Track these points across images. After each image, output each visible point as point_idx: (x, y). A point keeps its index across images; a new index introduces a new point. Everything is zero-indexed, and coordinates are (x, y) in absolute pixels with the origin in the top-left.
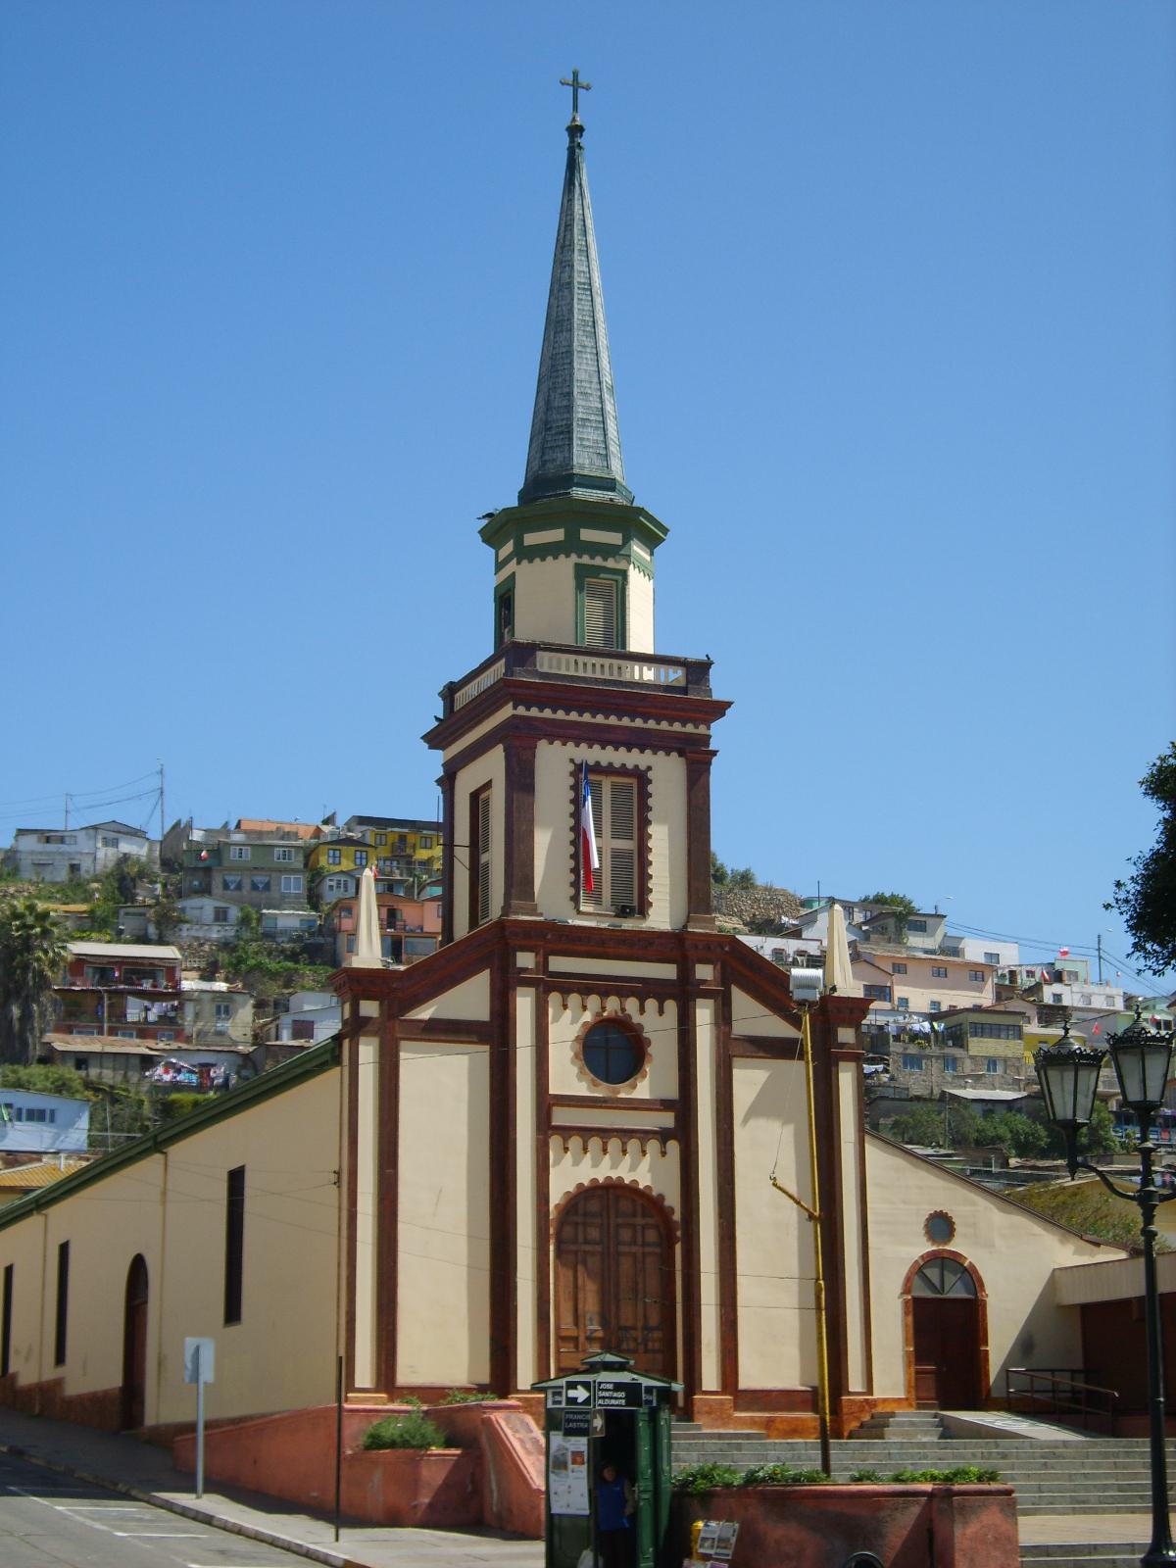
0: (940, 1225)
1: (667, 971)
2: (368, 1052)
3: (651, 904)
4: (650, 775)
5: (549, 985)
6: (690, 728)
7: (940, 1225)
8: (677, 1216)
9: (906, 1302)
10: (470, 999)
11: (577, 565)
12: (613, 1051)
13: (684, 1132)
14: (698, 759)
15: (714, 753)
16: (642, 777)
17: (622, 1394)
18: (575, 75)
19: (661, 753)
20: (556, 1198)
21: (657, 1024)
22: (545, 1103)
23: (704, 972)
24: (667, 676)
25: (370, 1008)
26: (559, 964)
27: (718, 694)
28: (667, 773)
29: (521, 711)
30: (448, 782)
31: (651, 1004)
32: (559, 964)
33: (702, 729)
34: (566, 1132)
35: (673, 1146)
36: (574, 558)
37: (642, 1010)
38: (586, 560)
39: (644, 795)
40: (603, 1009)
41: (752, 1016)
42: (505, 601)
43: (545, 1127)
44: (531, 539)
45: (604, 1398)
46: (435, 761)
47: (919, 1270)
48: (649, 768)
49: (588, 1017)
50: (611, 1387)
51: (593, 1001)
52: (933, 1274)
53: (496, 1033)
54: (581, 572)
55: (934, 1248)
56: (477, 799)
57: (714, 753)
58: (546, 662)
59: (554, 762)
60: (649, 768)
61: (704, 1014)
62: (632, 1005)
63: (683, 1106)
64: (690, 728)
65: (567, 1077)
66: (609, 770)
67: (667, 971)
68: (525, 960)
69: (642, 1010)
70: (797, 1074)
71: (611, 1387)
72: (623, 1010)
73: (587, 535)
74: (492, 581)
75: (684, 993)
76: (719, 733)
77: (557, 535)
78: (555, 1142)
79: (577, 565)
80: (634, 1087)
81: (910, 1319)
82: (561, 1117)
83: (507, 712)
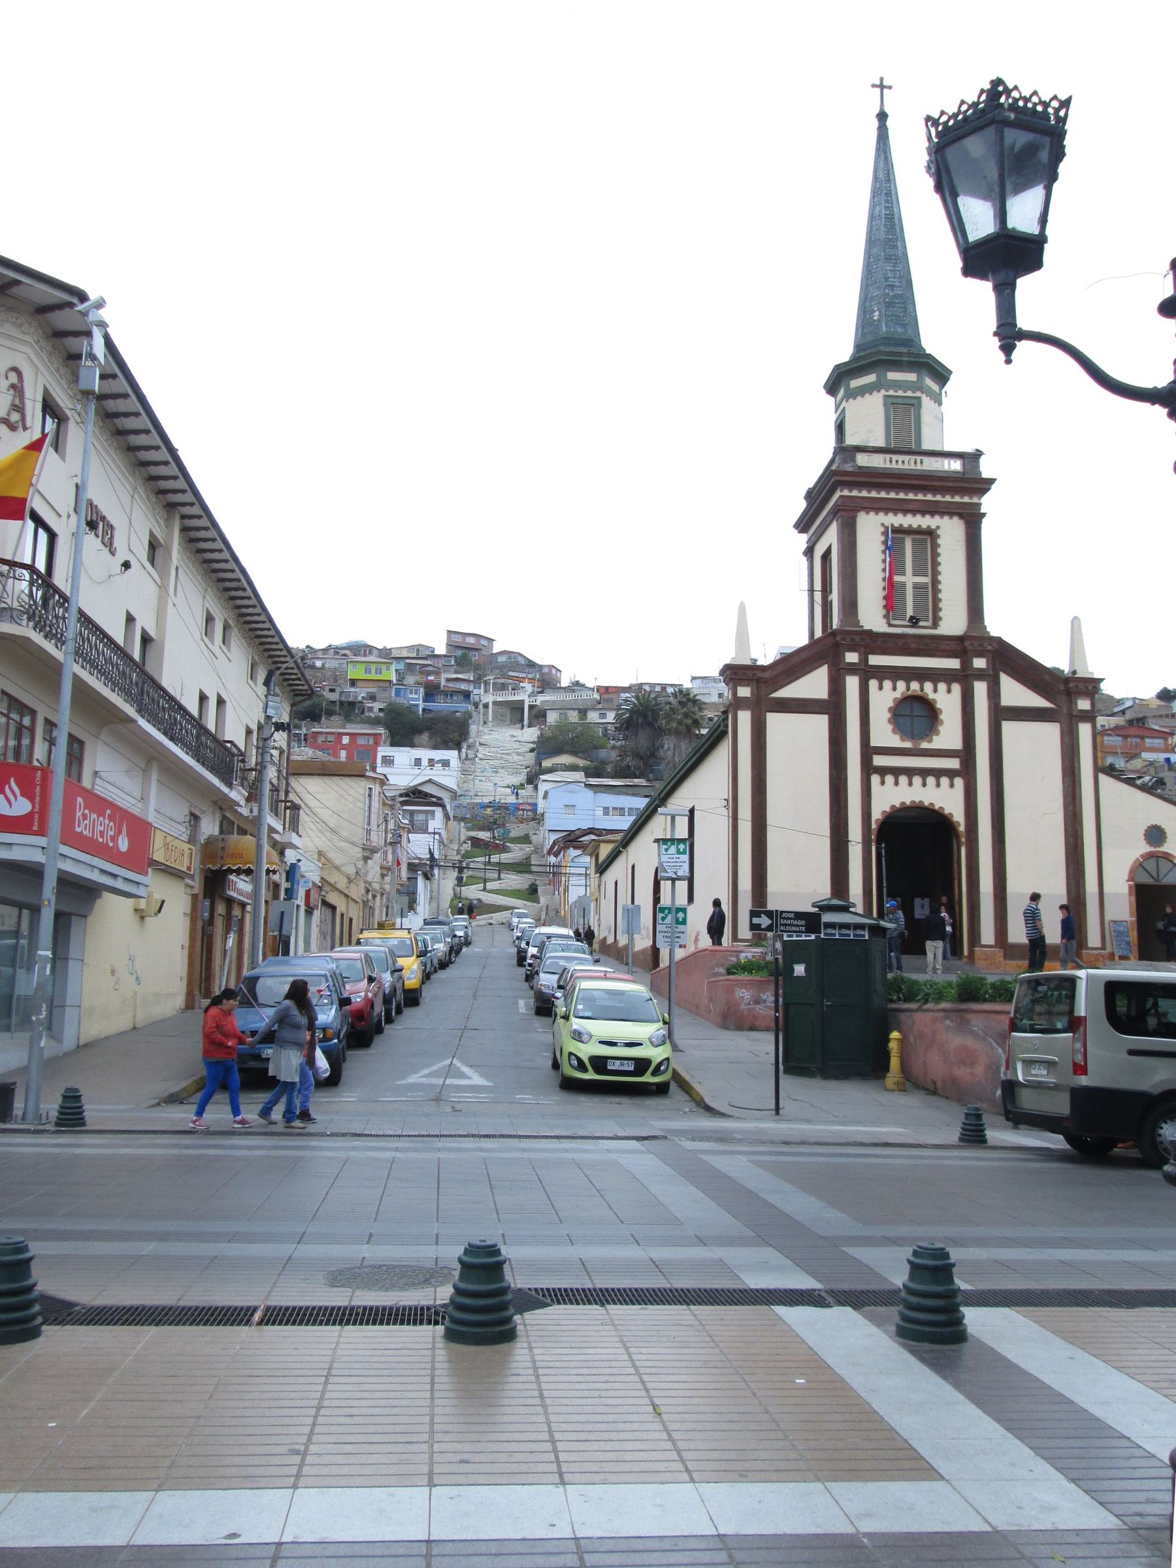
0: (1155, 834)
1: (954, 664)
2: (744, 718)
3: (941, 619)
4: (939, 532)
5: (867, 673)
6: (966, 499)
7: (1155, 834)
8: (962, 828)
9: (1130, 887)
10: (814, 684)
11: (886, 397)
12: (917, 715)
13: (968, 771)
14: (973, 520)
15: (984, 515)
16: (931, 534)
17: (803, 922)
18: (882, 79)
19: (946, 518)
20: (877, 815)
21: (947, 700)
22: (868, 751)
23: (980, 663)
24: (949, 464)
25: (744, 692)
26: (875, 660)
27: (985, 474)
28: (950, 531)
29: (846, 493)
30: (809, 552)
31: (942, 687)
32: (875, 660)
33: (975, 500)
34: (883, 771)
35: (959, 782)
36: (883, 392)
37: (935, 691)
38: (891, 393)
39: (935, 546)
40: (908, 689)
41: (1014, 693)
42: (840, 428)
43: (868, 769)
44: (855, 383)
45: (785, 925)
46: (802, 540)
47: (1139, 866)
48: (938, 527)
49: (898, 694)
50: (792, 915)
51: (901, 685)
52: (1151, 865)
53: (833, 707)
54: (889, 402)
55: (1152, 849)
56: (826, 556)
57: (984, 515)
58: (863, 460)
59: (870, 530)
60: (938, 527)
61: (980, 689)
62: (928, 687)
63: (967, 753)
64: (966, 499)
65: (883, 734)
66: (910, 531)
67: (954, 664)
68: (852, 657)
69: (935, 691)
70: (1050, 733)
71: (792, 915)
72: (922, 689)
73: (892, 376)
74: (832, 417)
75: (965, 678)
76: (988, 503)
77: (871, 378)
78: (875, 779)
79: (886, 397)
80: (930, 741)
81: (1133, 898)
82: (879, 761)
83: (838, 494)
